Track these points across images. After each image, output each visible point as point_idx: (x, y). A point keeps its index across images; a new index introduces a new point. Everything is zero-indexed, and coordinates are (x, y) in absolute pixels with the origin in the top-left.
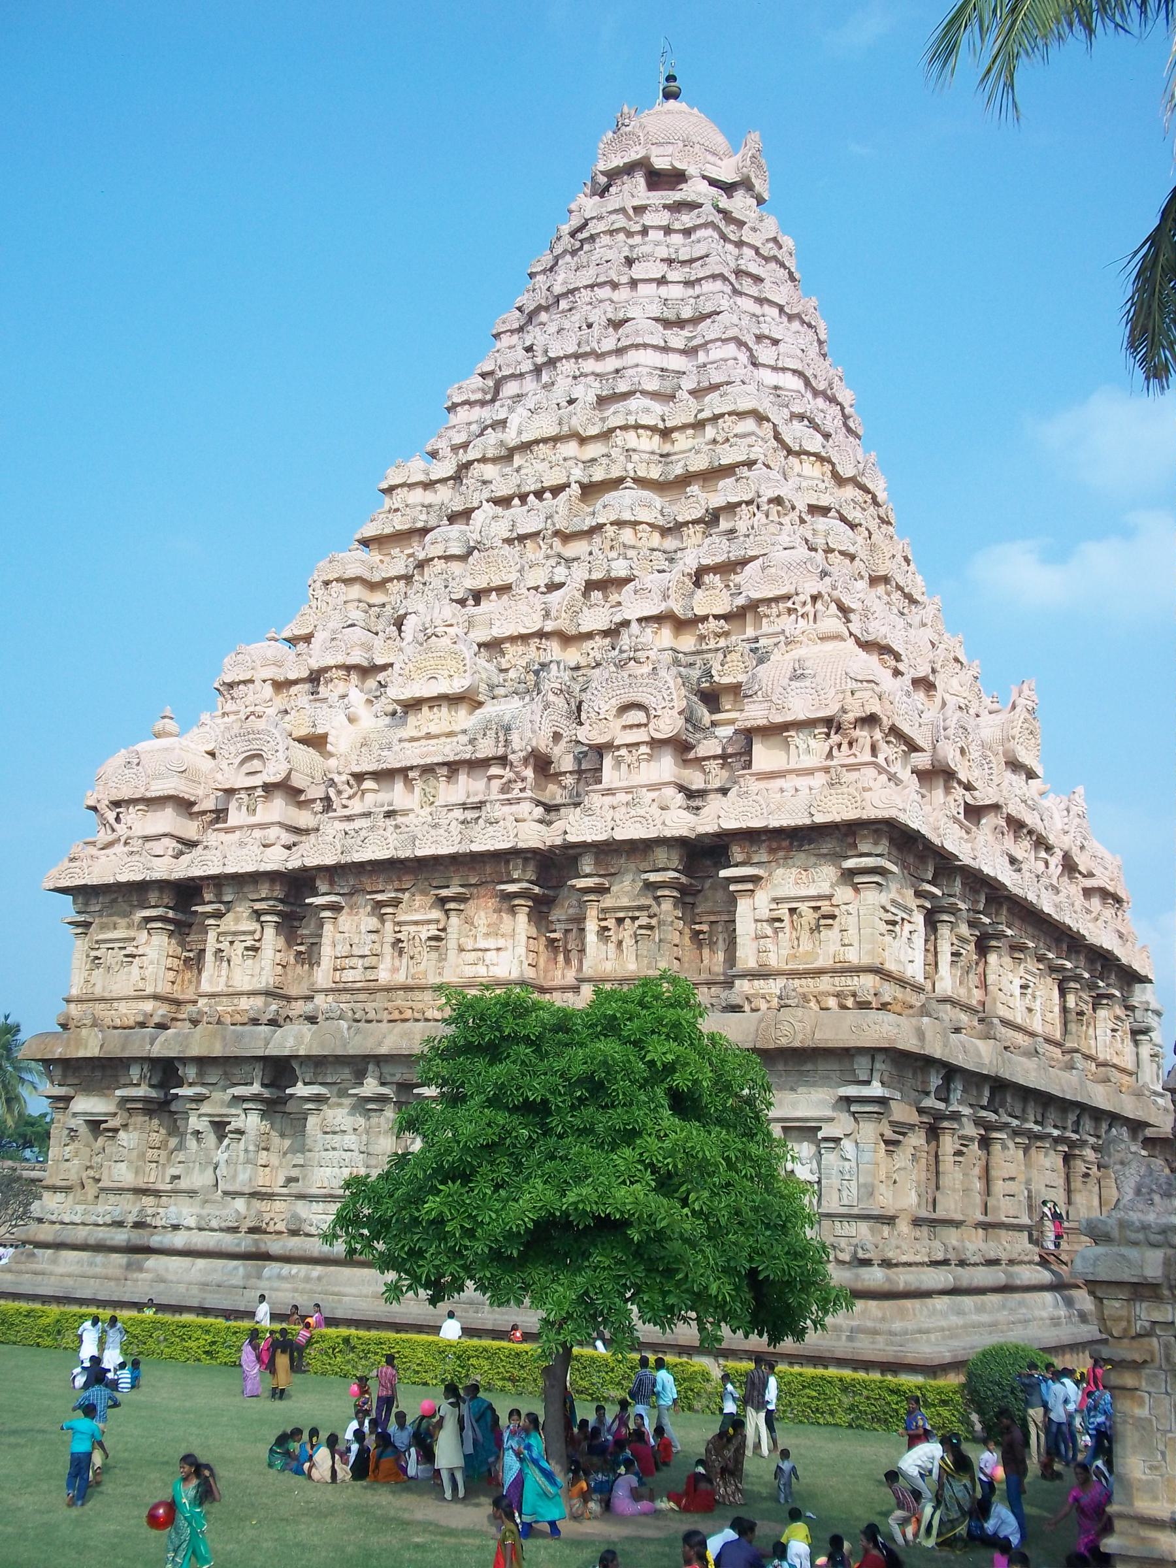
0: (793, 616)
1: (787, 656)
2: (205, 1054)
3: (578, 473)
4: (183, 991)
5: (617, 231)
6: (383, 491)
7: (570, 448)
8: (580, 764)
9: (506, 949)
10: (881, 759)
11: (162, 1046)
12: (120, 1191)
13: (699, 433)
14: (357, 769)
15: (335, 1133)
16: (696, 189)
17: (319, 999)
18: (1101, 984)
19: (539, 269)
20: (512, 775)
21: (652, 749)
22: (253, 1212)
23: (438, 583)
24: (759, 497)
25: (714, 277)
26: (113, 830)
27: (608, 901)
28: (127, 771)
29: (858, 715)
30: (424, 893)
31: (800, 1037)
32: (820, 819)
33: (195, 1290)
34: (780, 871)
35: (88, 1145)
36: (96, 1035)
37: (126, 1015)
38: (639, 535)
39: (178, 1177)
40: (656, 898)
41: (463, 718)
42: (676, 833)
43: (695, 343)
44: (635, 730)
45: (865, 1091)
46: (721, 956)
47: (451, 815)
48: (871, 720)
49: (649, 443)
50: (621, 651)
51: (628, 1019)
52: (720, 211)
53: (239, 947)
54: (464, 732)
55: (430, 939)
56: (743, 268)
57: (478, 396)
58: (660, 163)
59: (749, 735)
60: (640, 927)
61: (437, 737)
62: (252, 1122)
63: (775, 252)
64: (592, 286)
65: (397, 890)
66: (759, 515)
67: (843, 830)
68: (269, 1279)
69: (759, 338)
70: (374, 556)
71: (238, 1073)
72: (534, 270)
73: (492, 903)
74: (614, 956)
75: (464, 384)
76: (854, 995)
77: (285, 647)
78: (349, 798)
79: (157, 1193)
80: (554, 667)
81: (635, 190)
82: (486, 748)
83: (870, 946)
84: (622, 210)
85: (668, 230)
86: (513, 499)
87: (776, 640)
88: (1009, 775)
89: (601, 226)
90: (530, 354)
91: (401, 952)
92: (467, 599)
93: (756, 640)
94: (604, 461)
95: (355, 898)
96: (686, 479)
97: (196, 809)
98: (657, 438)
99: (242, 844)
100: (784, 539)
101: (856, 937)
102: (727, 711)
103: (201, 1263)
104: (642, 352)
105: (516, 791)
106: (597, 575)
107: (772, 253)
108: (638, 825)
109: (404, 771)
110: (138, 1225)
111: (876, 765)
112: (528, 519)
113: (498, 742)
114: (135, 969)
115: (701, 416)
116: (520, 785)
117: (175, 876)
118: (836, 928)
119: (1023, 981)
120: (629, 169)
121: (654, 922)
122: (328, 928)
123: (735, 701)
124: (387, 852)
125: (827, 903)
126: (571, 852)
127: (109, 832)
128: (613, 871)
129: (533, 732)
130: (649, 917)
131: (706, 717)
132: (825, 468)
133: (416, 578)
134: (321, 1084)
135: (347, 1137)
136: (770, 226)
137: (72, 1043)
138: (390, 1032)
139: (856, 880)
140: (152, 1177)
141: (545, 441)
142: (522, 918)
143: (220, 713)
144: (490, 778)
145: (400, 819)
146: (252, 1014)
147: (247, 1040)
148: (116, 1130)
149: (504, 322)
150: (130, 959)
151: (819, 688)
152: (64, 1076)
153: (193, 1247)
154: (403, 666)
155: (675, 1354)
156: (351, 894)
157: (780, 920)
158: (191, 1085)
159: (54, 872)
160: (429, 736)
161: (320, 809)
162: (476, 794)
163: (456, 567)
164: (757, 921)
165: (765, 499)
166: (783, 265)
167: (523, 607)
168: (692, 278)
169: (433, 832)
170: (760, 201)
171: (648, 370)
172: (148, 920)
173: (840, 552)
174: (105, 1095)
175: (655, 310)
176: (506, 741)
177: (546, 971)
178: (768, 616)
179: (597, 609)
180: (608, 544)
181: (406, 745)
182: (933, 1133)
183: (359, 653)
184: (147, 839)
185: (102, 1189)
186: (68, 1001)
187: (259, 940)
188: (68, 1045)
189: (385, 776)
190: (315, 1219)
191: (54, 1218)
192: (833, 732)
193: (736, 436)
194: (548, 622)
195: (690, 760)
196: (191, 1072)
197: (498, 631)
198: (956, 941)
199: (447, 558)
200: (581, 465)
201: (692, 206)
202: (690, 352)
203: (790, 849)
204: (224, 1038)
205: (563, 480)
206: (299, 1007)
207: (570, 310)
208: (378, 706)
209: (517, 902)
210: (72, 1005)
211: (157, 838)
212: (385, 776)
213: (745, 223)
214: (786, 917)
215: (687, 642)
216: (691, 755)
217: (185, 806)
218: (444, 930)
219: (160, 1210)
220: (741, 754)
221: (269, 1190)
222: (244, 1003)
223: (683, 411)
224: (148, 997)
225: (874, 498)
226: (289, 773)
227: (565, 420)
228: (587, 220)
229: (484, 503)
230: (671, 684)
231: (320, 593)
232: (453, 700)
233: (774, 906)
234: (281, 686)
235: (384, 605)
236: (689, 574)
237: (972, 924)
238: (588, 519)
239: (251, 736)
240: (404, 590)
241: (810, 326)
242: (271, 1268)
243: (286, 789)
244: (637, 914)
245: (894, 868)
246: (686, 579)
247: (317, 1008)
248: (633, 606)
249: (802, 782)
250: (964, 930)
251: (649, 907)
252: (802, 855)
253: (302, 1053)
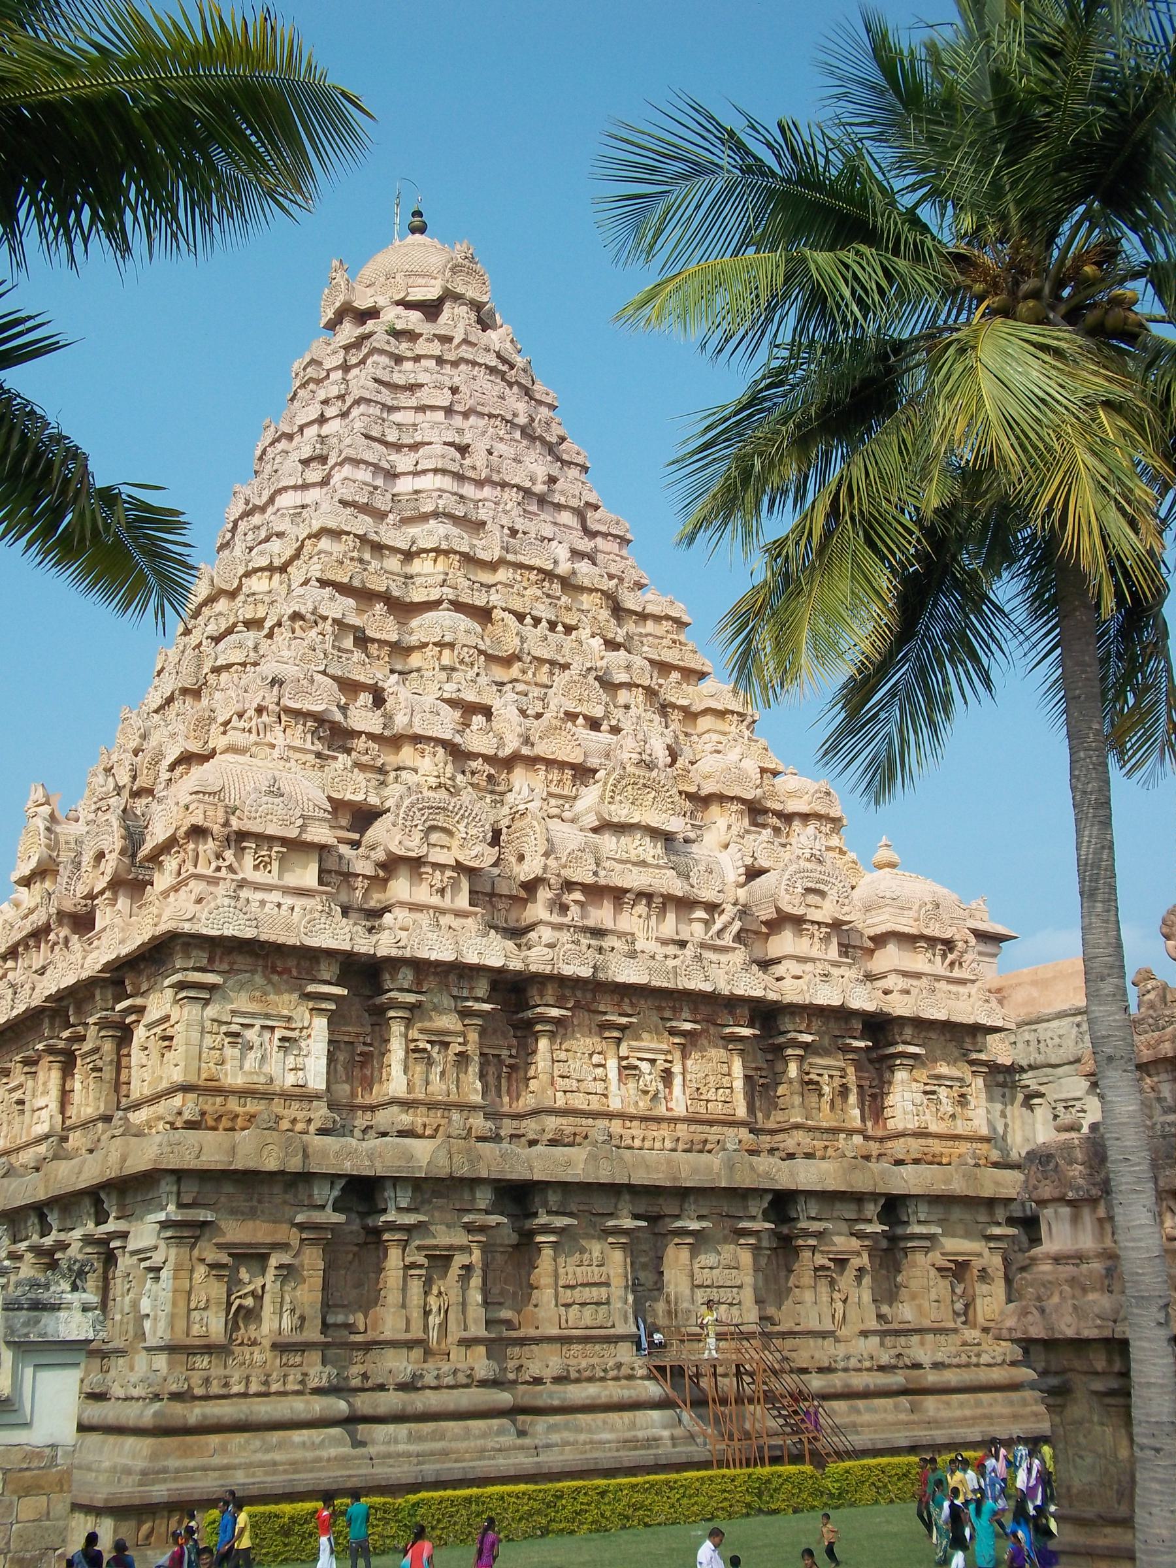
5: (307, 383)
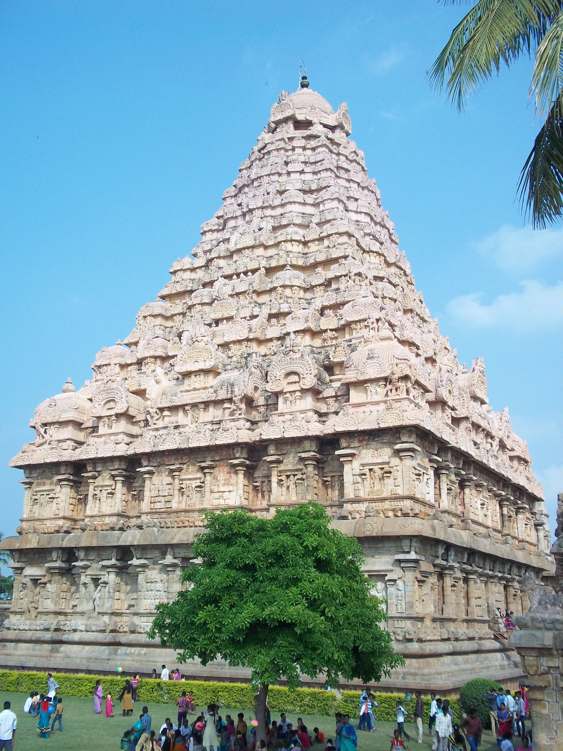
0: (368, 329)
1: (365, 348)
2: (89, 545)
3: (264, 263)
4: (77, 515)
5: (281, 149)
6: (171, 273)
7: (260, 251)
8: (267, 401)
9: (233, 491)
10: (411, 396)
11: (67, 542)
12: (48, 613)
13: (321, 243)
14: (160, 406)
15: (152, 582)
16: (317, 129)
17: (144, 517)
18: (519, 502)
19: (244, 167)
20: (235, 407)
21: (301, 393)
22: (112, 622)
23: (198, 316)
24: (350, 273)
25: (326, 170)
26: (43, 437)
27: (282, 467)
28: (50, 409)
29: (400, 375)
30: (194, 465)
31: (376, 531)
32: (383, 425)
33: (84, 662)
34: (364, 451)
35: (32, 591)
36: (35, 537)
37: (50, 527)
38: (294, 292)
39: (76, 606)
40: (305, 465)
41: (211, 381)
42: (314, 434)
43: (318, 201)
44: (293, 385)
45: (408, 557)
46: (337, 492)
47: (206, 427)
48: (406, 378)
49: (297, 248)
50: (286, 347)
51: (293, 525)
52: (329, 139)
53: (105, 493)
54: (212, 387)
55: (197, 487)
56: (340, 165)
57: (216, 227)
58: (300, 117)
59: (348, 386)
60: (298, 479)
62: (111, 578)
63: (355, 158)
64: (269, 175)
65: (180, 464)
66: (350, 281)
67: (394, 430)
68: (121, 655)
69: (349, 198)
70: (167, 304)
71: (104, 554)
72: (241, 168)
73: (226, 469)
74: (285, 494)
75: (209, 222)
76: (401, 510)
77: (126, 348)
78: (157, 420)
79: (65, 614)
80: (254, 355)
81: (289, 130)
82: (222, 395)
83: (408, 486)
84: (283, 139)
85: (304, 148)
86: (233, 275)
87: (360, 341)
88: (472, 403)
90: (240, 207)
91: (183, 494)
92: (212, 324)
93: (350, 340)
94: (276, 257)
95: (160, 468)
96: (315, 265)
97: (83, 426)
98: (301, 246)
99: (105, 443)
100: (363, 293)
101: (402, 482)
102: (337, 375)
103: (87, 648)
104: (293, 205)
105: (237, 415)
106: (274, 311)
107: (354, 158)
108: (296, 430)
109: (182, 407)
110: (56, 630)
111: (409, 399)
112: (240, 285)
113: (228, 391)
114: (54, 504)
115: (321, 235)
116: (239, 412)
117: (73, 459)
118: (392, 478)
119: (482, 502)
120: (286, 120)
121: (304, 476)
122: (147, 482)
123: (341, 370)
124: (175, 446)
125: (387, 466)
126: (264, 444)
127: (41, 438)
128: (284, 452)
129: (245, 386)
130: (302, 474)
131: (327, 378)
132: (381, 259)
133: (188, 314)
134: (145, 559)
135: (158, 584)
136: (353, 146)
137: (24, 541)
138: (178, 532)
139: (401, 455)
140: (63, 606)
141: (248, 248)
142: (241, 476)
143: (94, 380)
144: (224, 409)
145: (181, 430)
146: (111, 525)
147: (109, 538)
148: (45, 584)
149: (228, 193)
151: (381, 363)
152: (20, 557)
153: (83, 640)
154: (182, 356)
155: (319, 687)
156: (158, 466)
157: (365, 475)
158: (82, 560)
159: (14, 458)
160: (195, 389)
161: (143, 425)
162: (217, 417)
163: (207, 308)
164: (354, 475)
165: (353, 274)
166: (359, 164)
167: (239, 327)
168: (316, 171)
169: (197, 435)
170: (348, 134)
171: (297, 214)
172: (60, 480)
173: (389, 298)
174: (40, 566)
175: (299, 186)
176: (232, 391)
177: (253, 502)
178: (356, 329)
179: (274, 327)
180: (279, 296)
181: (184, 394)
182: (441, 576)
183: (161, 350)
184: (60, 441)
185: (39, 613)
186: (22, 521)
187: (114, 489)
188: (22, 542)
189: (174, 409)
190: (143, 625)
191: (15, 627)
192: (388, 384)
193: (338, 244)
194: (251, 334)
195: (320, 399)
196: (82, 554)
197: (227, 339)
198: (449, 483)
199: (202, 304)
200: (265, 259)
201: (316, 137)
202: (316, 205)
203: (369, 440)
204: (98, 537)
205: (257, 266)
206: (134, 521)
207: (259, 186)
208: (170, 375)
209: (238, 468)
210: (24, 523)
211: (65, 441)
212: (174, 409)
213: (340, 145)
214: (368, 473)
215: (318, 342)
216: (321, 396)
217: (78, 425)
218: (203, 482)
219: (67, 622)
220: (344, 395)
221: (120, 611)
222: (107, 520)
223: (313, 233)
224: (60, 518)
225: (405, 272)
226: (128, 408)
227: (258, 238)
228: (266, 144)
229: (220, 278)
230: (310, 362)
231: (142, 322)
232: (206, 372)
233: (362, 468)
234: (123, 366)
235: (172, 327)
236: (318, 310)
237: (457, 475)
238: (269, 284)
239: (109, 391)
240: (182, 320)
241: (372, 192)
242: (121, 650)
243: (127, 416)
244: (296, 473)
245: (419, 449)
246: (316, 312)
247: (142, 522)
248: (291, 325)
249: (374, 408)
250: (453, 477)
251: (302, 470)
252: (375, 443)
253: (135, 544)
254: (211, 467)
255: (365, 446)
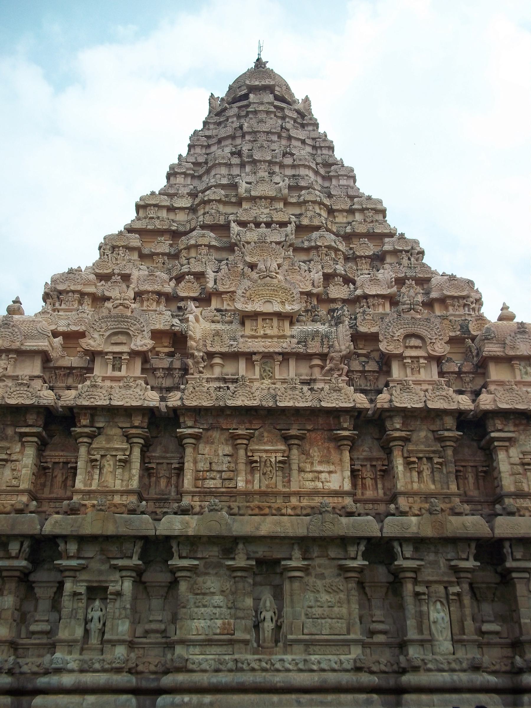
5: (271, 112)
8: (364, 366)
9: (335, 472)
34: (522, 437)
44: (414, 349)
55: (280, 462)
61: (271, 337)
64: (268, 133)
82: (314, 347)
85: (295, 121)
89: (262, 108)
91: (253, 470)
95: (210, 433)
108: (442, 401)
109: (249, 356)
122: (189, 451)
128: (411, 429)
141: (266, 198)
150: (4, 463)
158: (69, 558)
196: (73, 548)
199: (210, 246)
205: (287, 220)
207: (254, 141)
222: (117, 499)
232: (280, 316)
251: (441, 452)
254: (301, 438)
255: (521, 432)
